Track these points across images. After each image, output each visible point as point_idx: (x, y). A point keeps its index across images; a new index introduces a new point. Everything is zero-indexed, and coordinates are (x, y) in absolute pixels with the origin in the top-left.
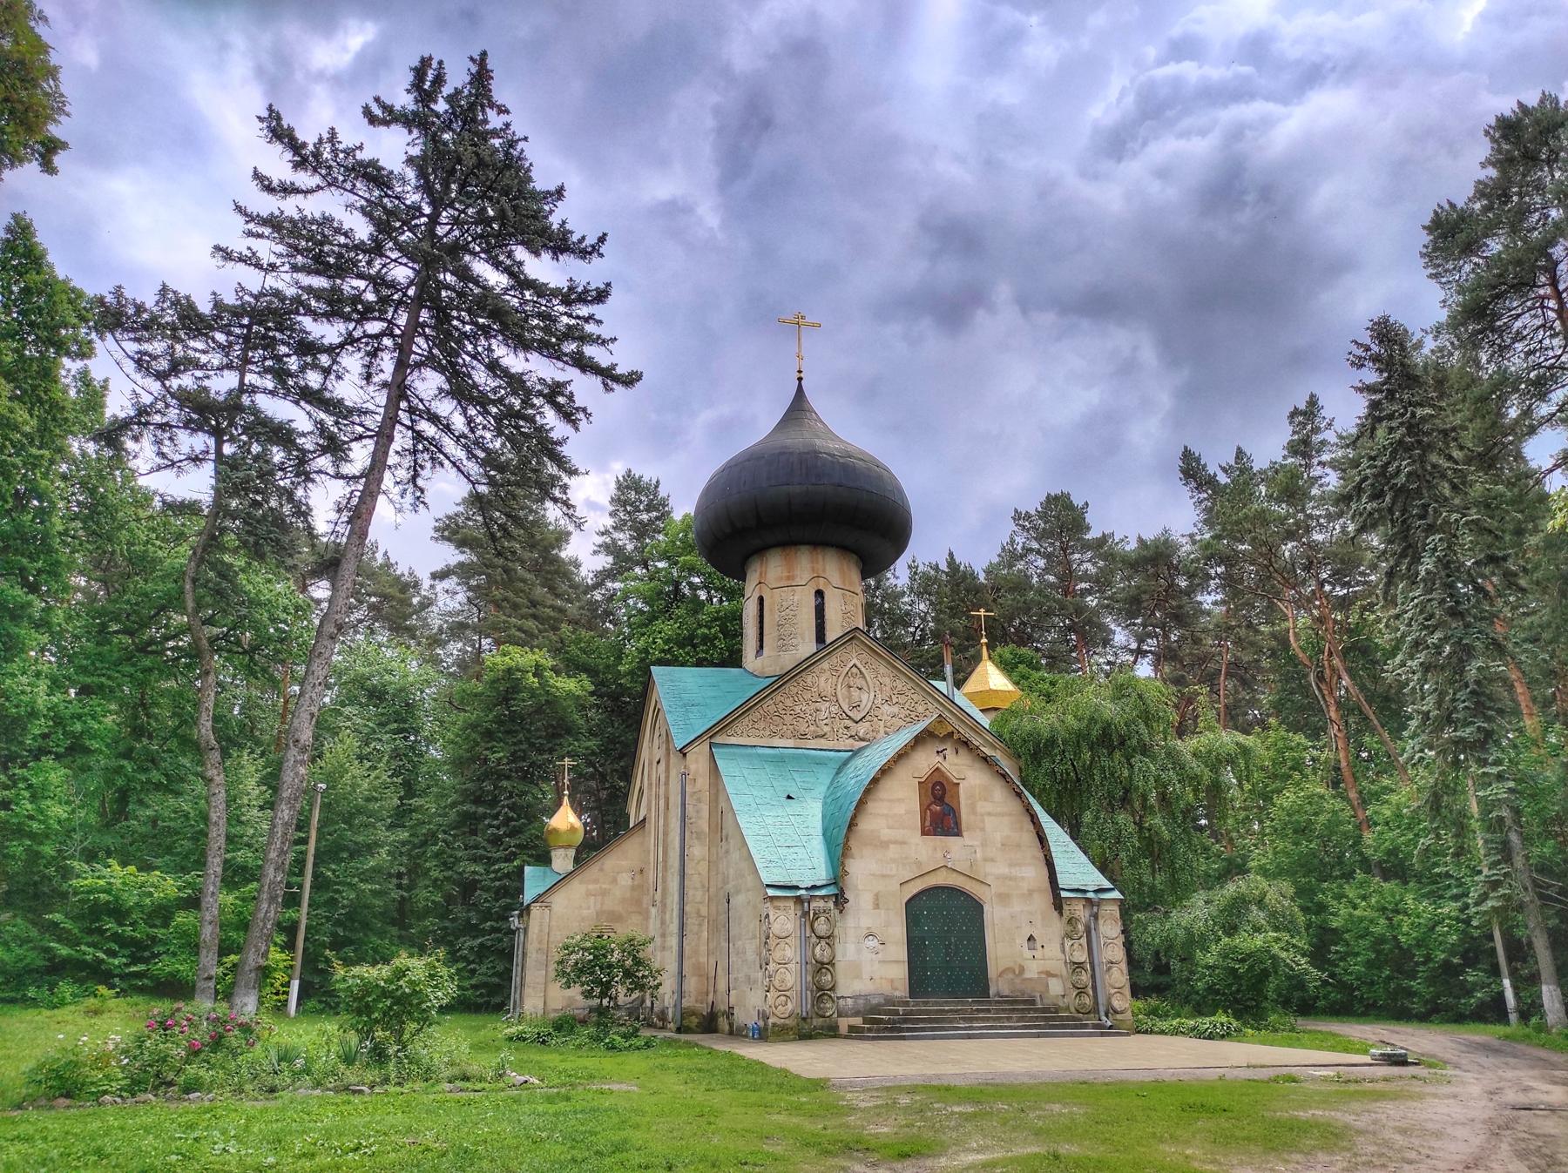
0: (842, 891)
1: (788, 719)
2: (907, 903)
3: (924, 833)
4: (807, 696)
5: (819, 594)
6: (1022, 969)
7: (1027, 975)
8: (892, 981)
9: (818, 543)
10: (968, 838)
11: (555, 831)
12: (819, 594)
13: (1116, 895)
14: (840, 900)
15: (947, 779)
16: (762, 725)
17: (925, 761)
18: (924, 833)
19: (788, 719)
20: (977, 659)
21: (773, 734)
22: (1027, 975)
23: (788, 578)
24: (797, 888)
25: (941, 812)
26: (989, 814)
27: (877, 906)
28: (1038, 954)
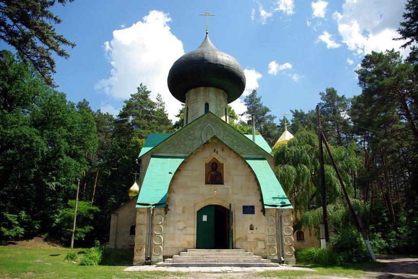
0: (167, 206)
1: (182, 146)
2: (198, 212)
3: (207, 183)
4: (190, 138)
5: (207, 105)
6: (246, 238)
7: (249, 240)
8: (188, 242)
9: (207, 85)
10: (226, 185)
11: (131, 191)
12: (207, 105)
13: (291, 207)
14: (166, 209)
15: (219, 162)
16: (172, 149)
17: (208, 155)
18: (207, 183)
19: (182, 146)
20: (284, 130)
21: (176, 152)
22: (249, 240)
23: (196, 99)
24: (148, 205)
25: (215, 175)
26: (236, 175)
27: (183, 212)
28: (254, 231)
